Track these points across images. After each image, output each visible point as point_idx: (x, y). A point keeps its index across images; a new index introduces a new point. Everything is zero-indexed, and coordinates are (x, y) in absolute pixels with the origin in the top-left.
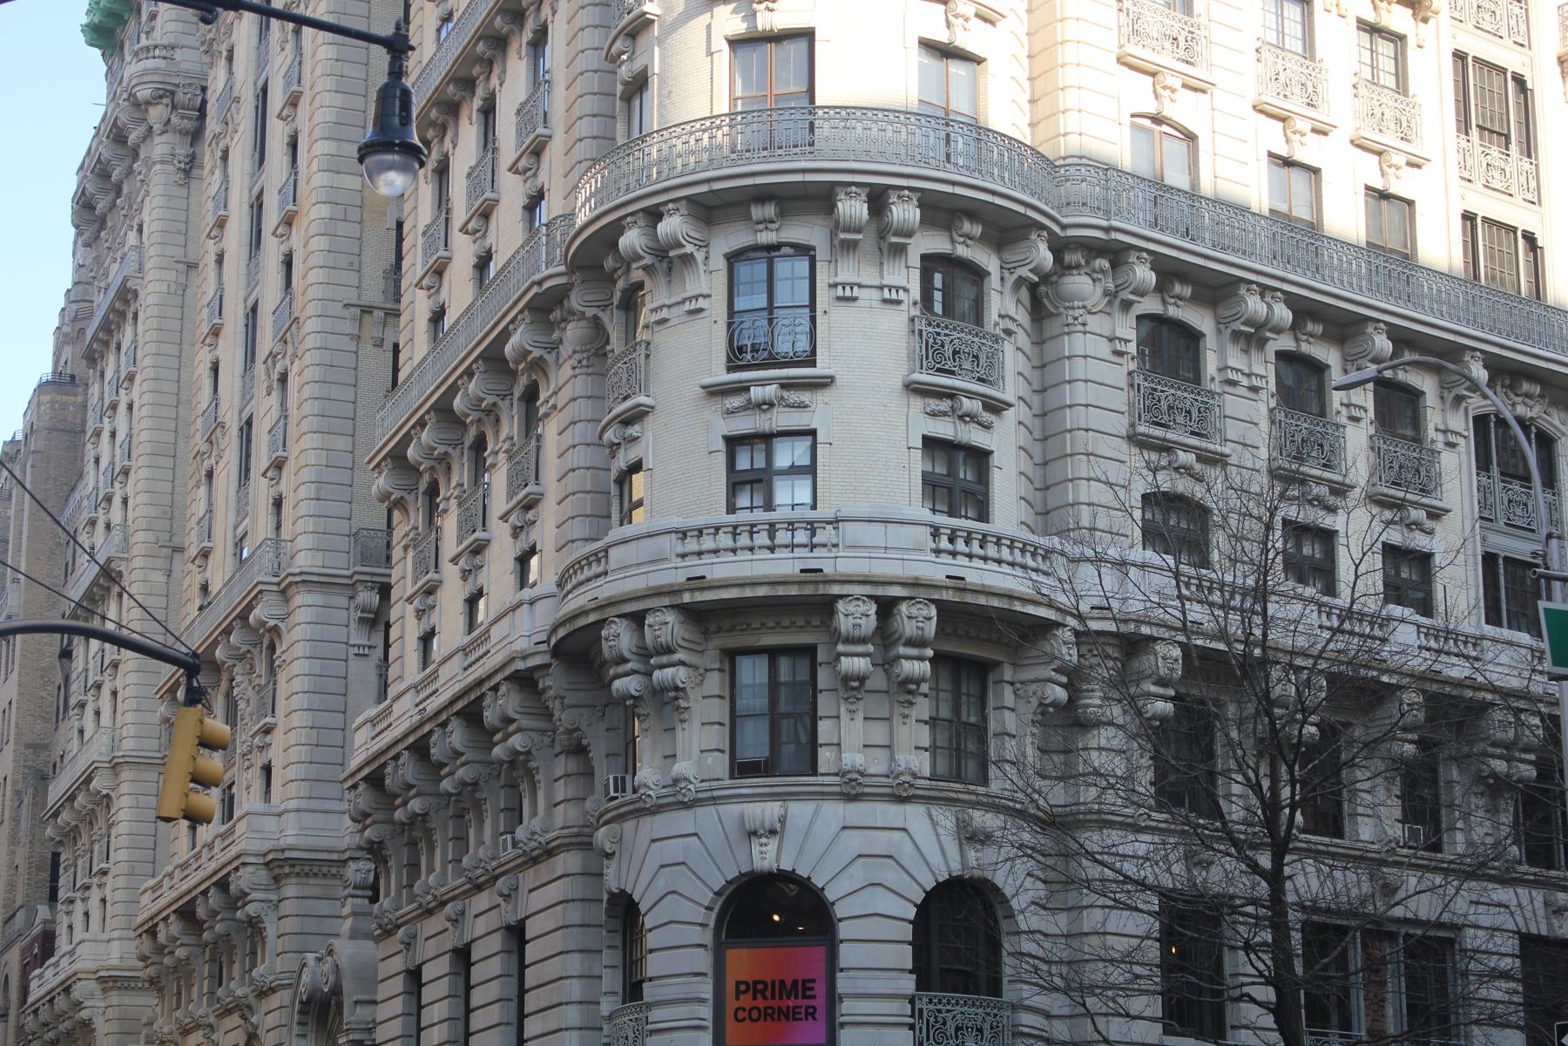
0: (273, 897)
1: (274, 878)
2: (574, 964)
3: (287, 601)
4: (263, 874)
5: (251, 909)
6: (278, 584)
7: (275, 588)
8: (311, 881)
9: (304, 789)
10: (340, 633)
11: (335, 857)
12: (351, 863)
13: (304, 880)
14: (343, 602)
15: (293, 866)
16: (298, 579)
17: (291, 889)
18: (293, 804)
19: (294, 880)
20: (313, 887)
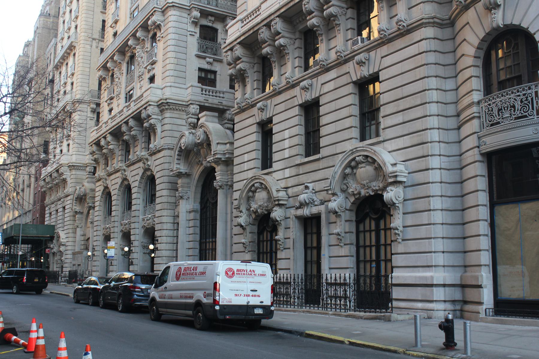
0: (160, 118)
1: (161, 111)
2: (433, 83)
3: (164, 16)
4: (157, 110)
5: (152, 121)
6: (161, 9)
7: (160, 10)
8: (175, 112)
9: (172, 79)
10: (184, 26)
11: (184, 103)
12: (191, 105)
13: (172, 111)
14: (186, 15)
15: (169, 106)
16: (171, 5)
17: (167, 114)
18: (169, 84)
19: (169, 111)
20: (175, 114)
